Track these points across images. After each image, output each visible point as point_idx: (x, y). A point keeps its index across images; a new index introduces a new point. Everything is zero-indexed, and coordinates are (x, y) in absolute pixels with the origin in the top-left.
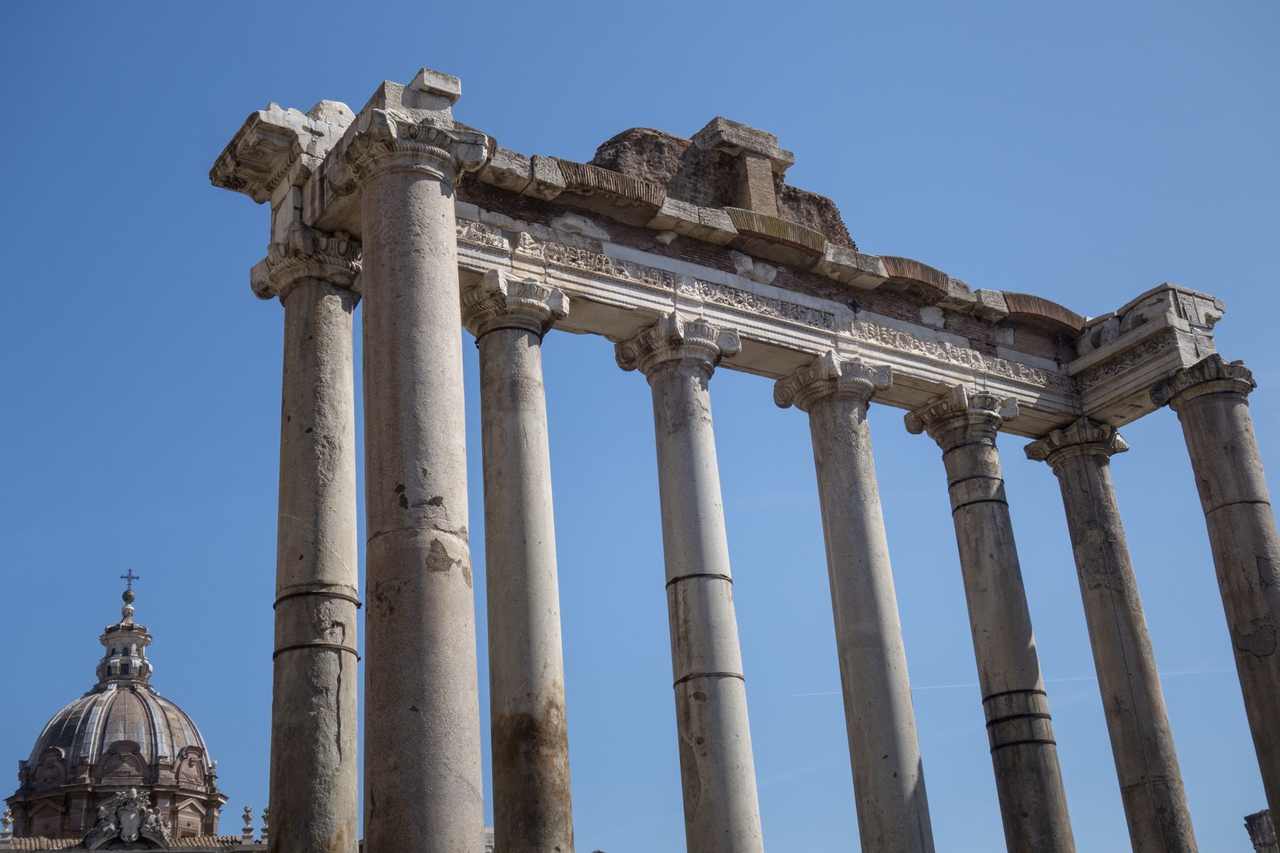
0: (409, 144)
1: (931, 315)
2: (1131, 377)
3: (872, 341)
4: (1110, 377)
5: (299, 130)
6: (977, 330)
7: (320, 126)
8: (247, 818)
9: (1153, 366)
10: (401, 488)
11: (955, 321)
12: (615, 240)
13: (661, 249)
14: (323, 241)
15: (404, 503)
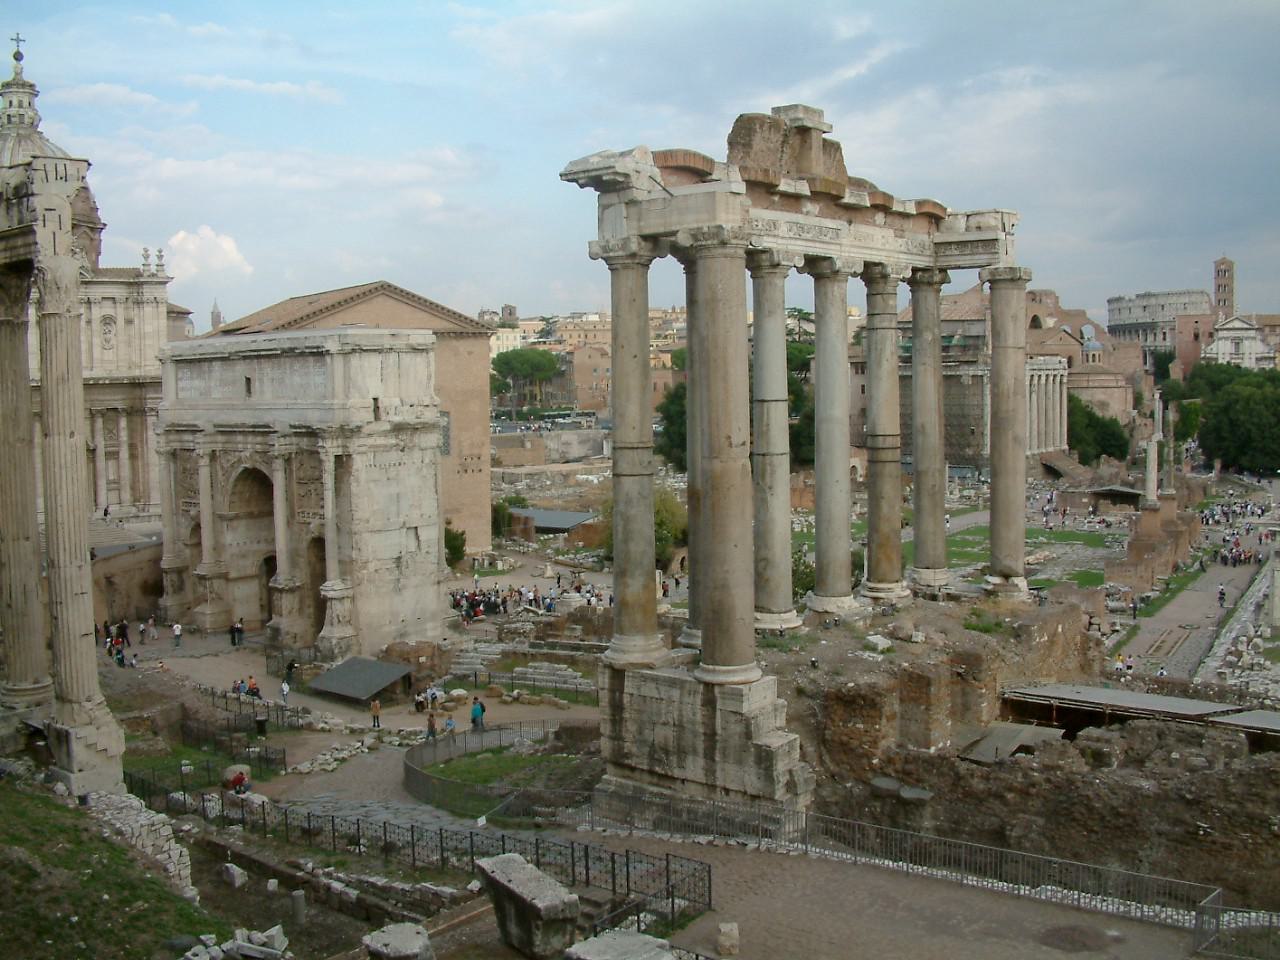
0: (734, 241)
1: (880, 217)
2: (969, 257)
3: (857, 243)
4: (957, 252)
5: (632, 173)
6: (898, 222)
7: (640, 167)
8: (146, 257)
9: (986, 256)
10: (729, 437)
11: (890, 219)
12: (755, 205)
13: (771, 206)
14: (643, 243)
15: (731, 445)
